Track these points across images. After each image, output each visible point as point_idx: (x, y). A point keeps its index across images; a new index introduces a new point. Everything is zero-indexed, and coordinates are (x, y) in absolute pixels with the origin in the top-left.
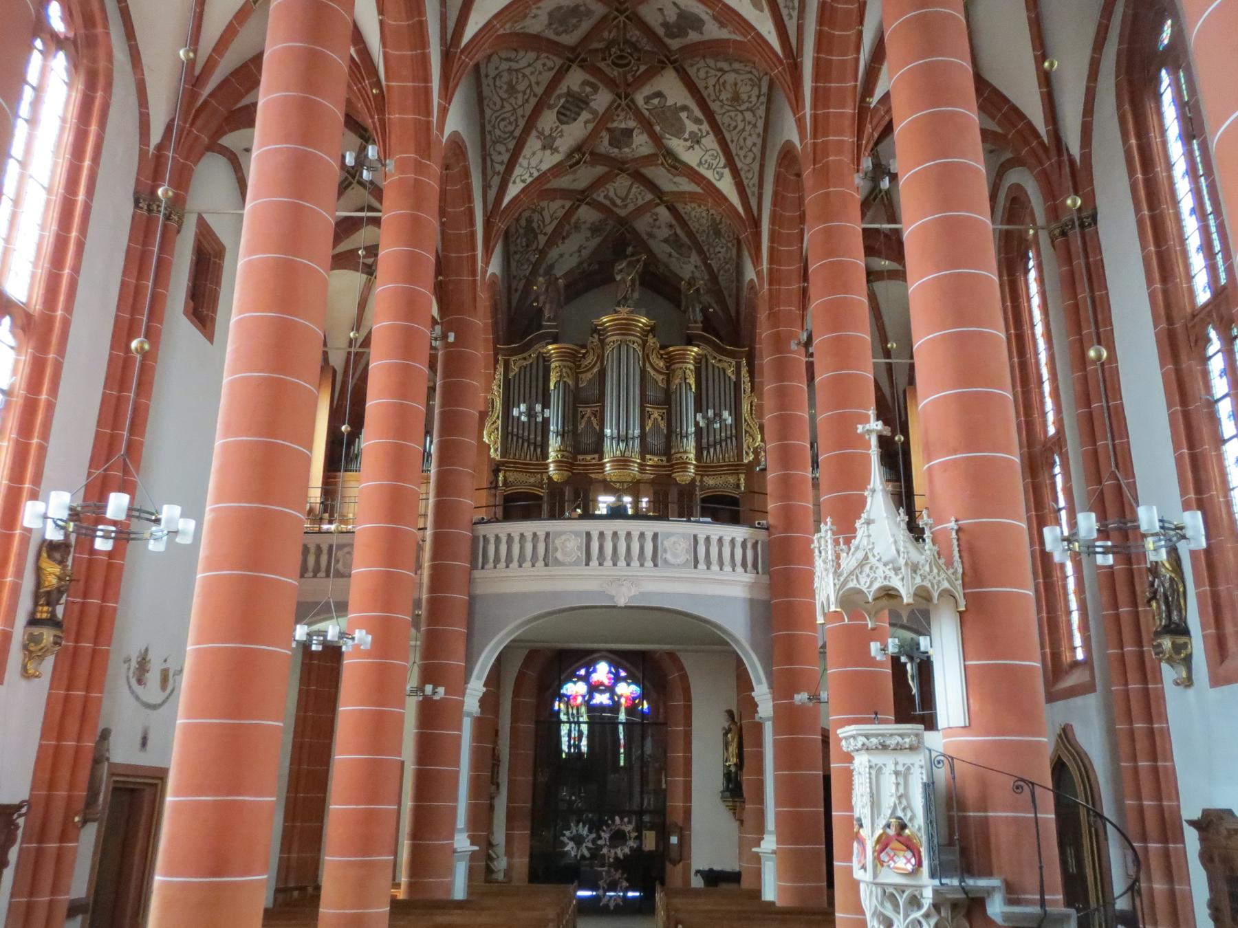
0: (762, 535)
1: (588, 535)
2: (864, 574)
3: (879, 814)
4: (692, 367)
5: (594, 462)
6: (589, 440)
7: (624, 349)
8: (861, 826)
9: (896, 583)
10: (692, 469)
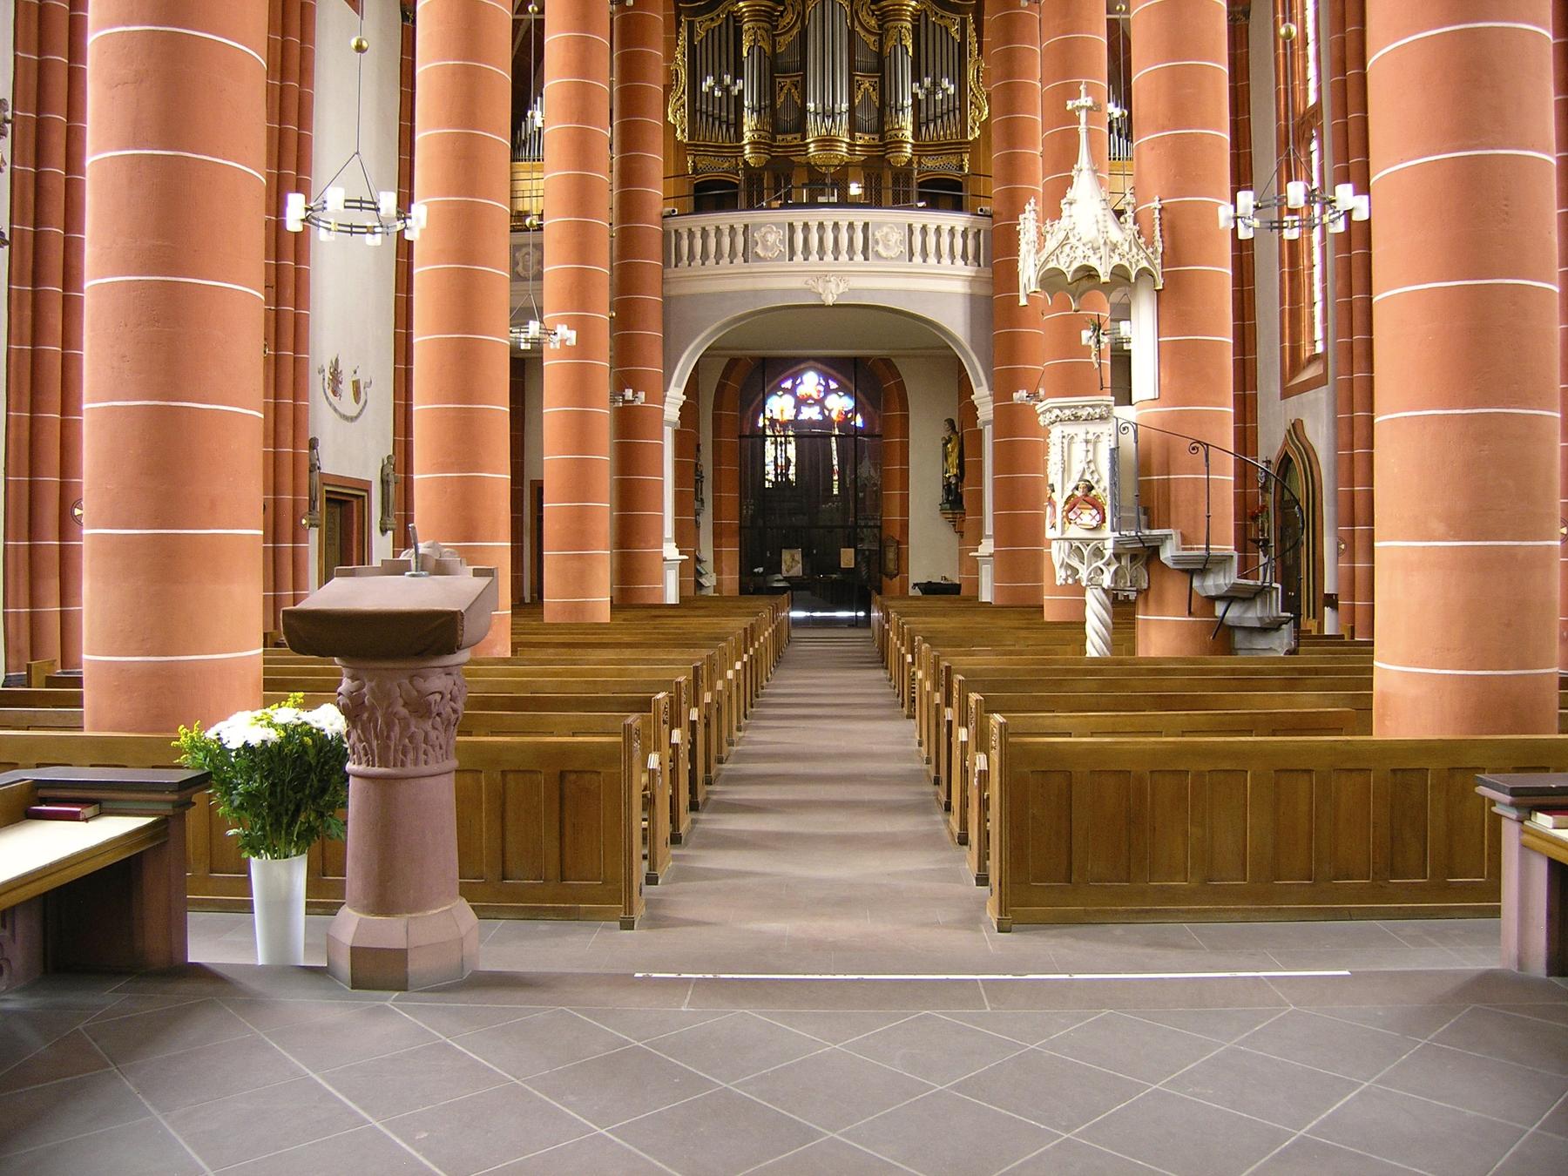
0: (984, 223)
1: (791, 225)
2: (1064, 254)
3: (1069, 479)
4: (909, 26)
5: (795, 142)
6: (787, 117)
8: (1053, 491)
9: (1093, 262)
10: (908, 149)
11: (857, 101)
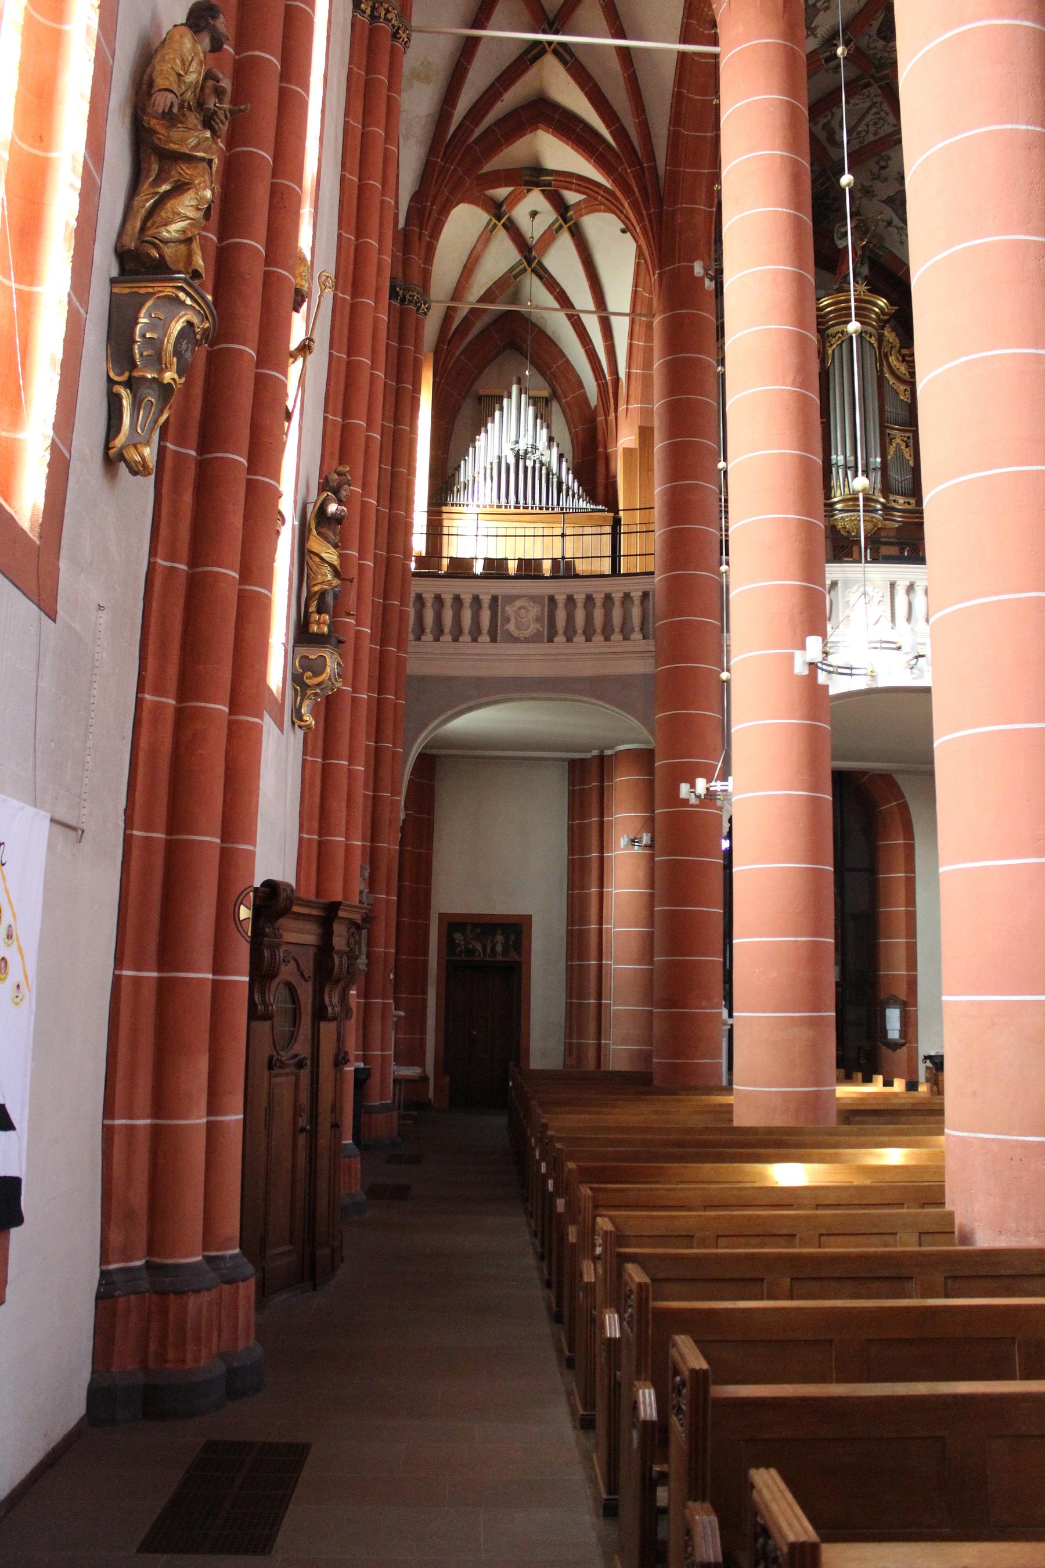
11: (889, 457)
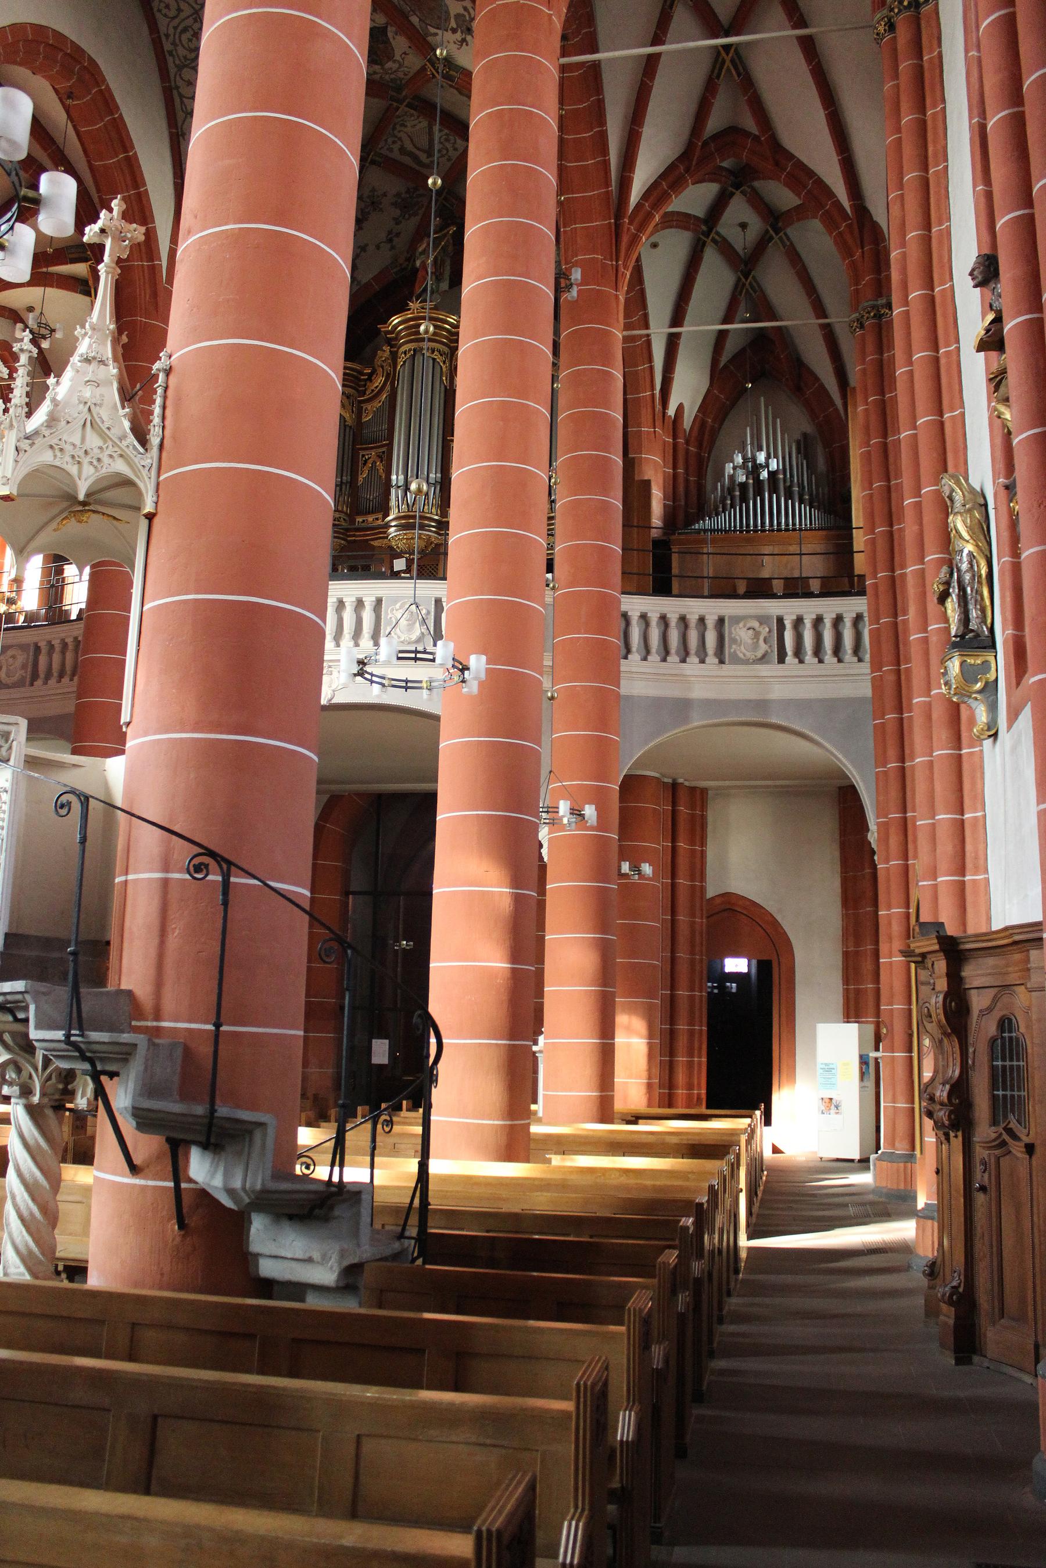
6: (372, 495)
7: (418, 359)
